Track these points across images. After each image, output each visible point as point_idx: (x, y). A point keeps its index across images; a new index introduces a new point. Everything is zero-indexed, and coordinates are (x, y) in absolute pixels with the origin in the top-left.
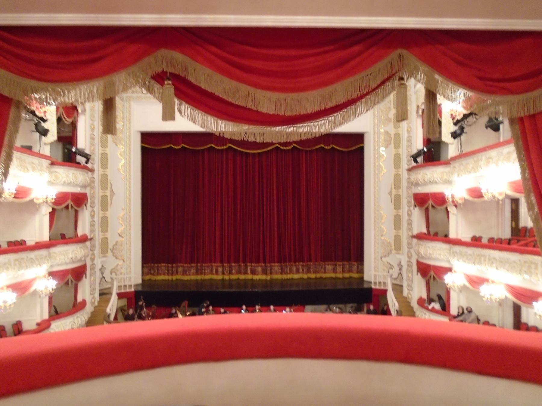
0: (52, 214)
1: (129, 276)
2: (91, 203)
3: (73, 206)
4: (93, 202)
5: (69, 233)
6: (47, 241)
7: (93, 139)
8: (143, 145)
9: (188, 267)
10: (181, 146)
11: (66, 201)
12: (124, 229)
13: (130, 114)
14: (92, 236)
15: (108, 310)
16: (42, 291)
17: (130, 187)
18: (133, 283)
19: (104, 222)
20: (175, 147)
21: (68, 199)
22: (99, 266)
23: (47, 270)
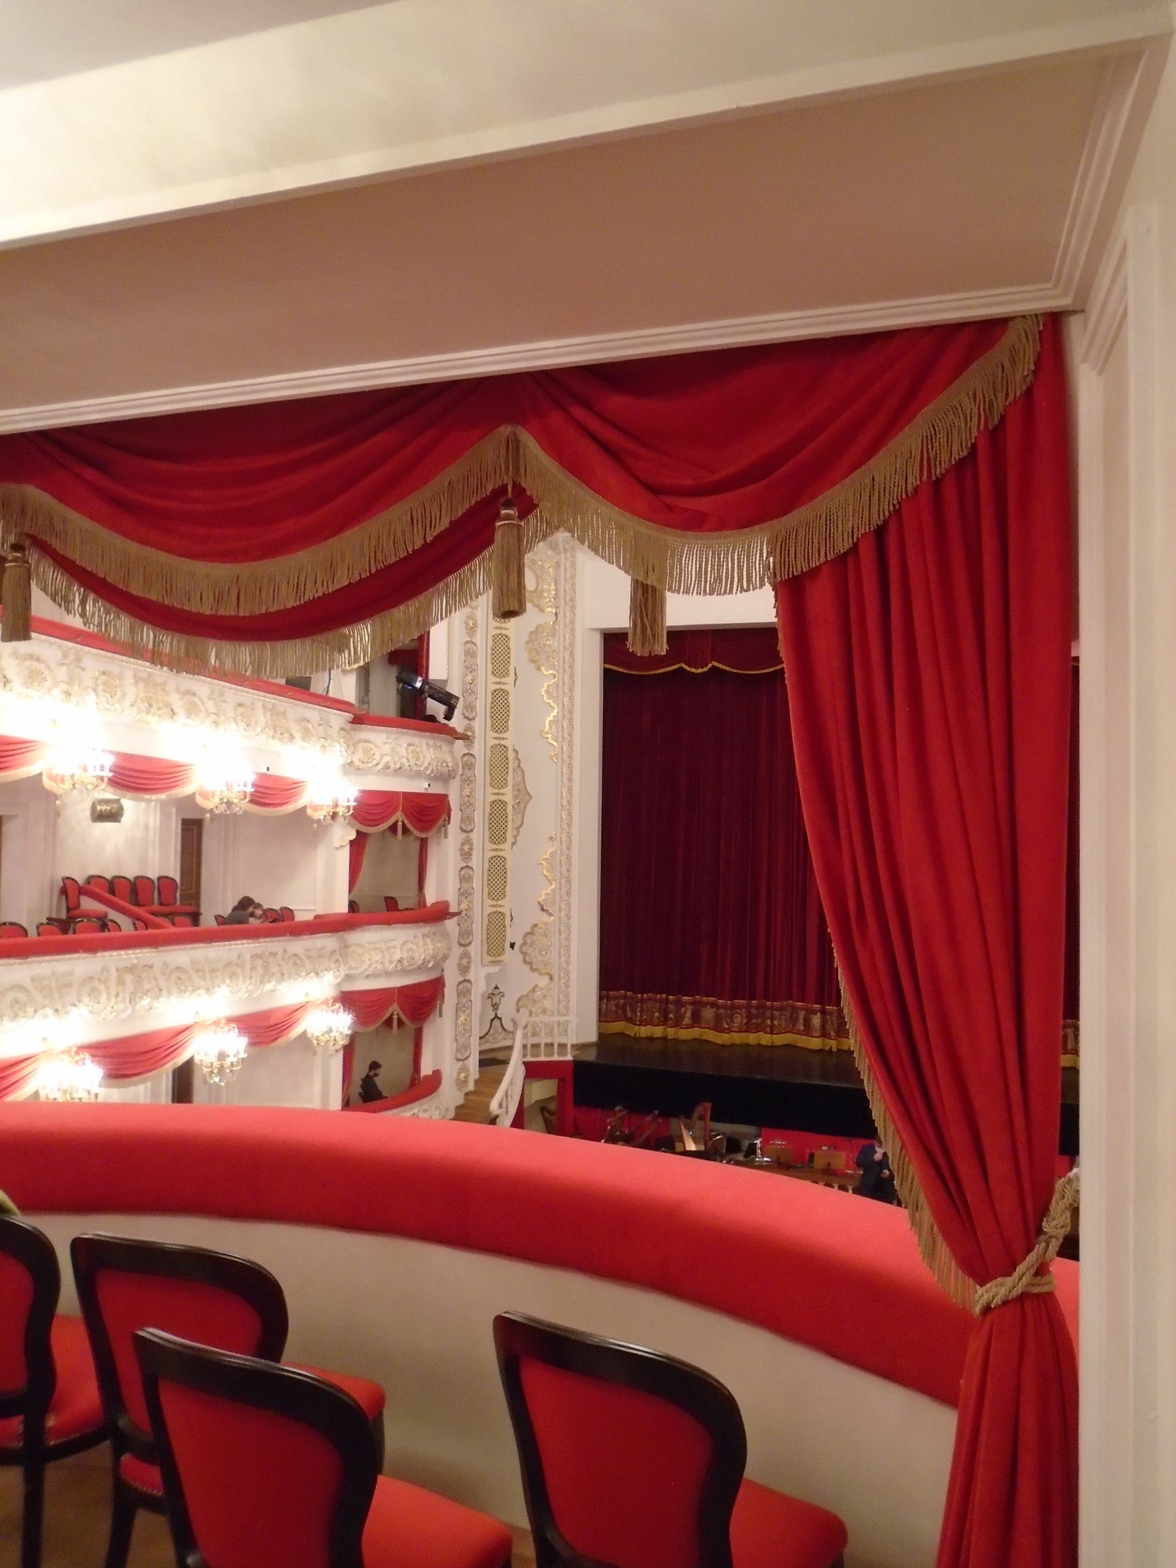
0: (357, 846)
1: (562, 1019)
2: (462, 820)
3: (409, 826)
4: (467, 820)
5: (406, 898)
6: (341, 914)
7: (470, 654)
8: (608, 666)
9: (724, 1007)
10: (710, 666)
11: (391, 814)
12: (554, 890)
13: (573, 584)
14: (463, 906)
15: (494, 1106)
16: (317, 1038)
17: (570, 780)
18: (572, 1039)
19: (497, 871)
20: (693, 670)
21: (395, 810)
22: (480, 987)
23: (339, 985)
